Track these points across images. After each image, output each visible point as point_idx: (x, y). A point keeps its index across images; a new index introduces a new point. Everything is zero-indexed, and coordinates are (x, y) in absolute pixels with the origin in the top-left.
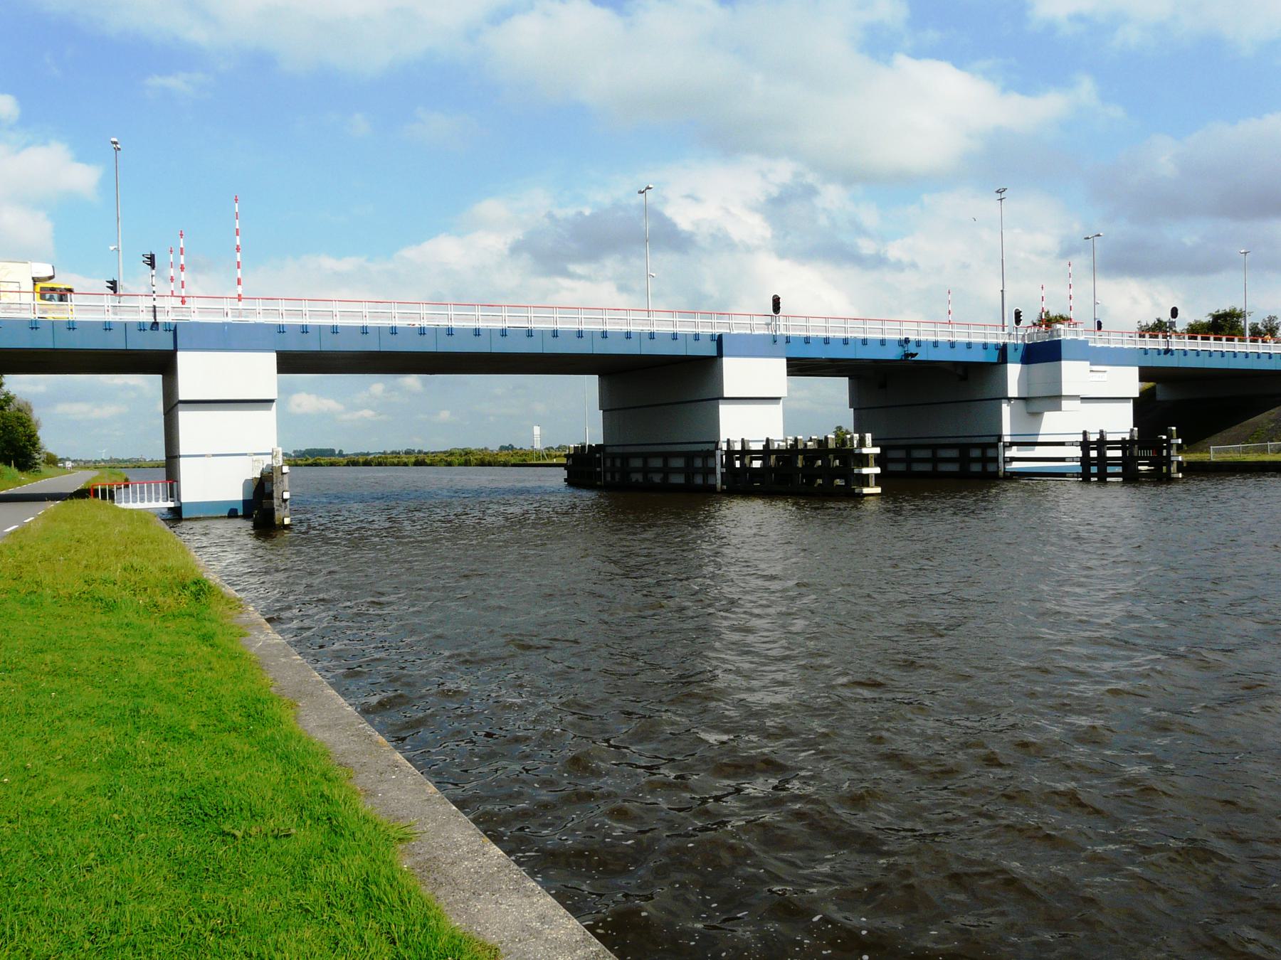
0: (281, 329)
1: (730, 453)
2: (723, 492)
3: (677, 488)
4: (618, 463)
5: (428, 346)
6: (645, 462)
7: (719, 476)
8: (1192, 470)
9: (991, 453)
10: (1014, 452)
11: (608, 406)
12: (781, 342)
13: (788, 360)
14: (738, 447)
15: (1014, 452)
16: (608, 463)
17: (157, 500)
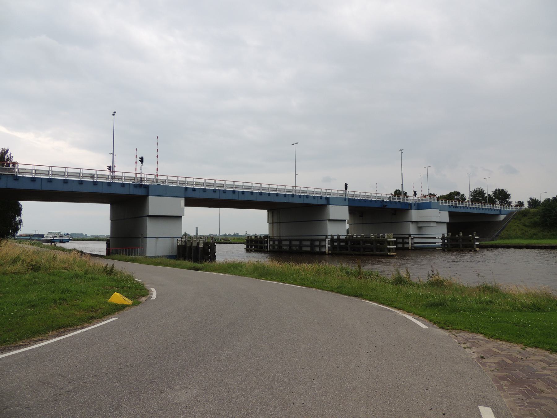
0: (186, 189)
1: (333, 240)
2: (329, 254)
3: (307, 253)
4: (276, 243)
5: (216, 196)
6: (403, 240)
7: (327, 248)
8: (482, 247)
9: (406, 240)
10: (416, 240)
11: (271, 223)
12: (347, 200)
13: (449, 212)
14: (335, 237)
15: (416, 240)
16: (271, 243)
17: (129, 255)
